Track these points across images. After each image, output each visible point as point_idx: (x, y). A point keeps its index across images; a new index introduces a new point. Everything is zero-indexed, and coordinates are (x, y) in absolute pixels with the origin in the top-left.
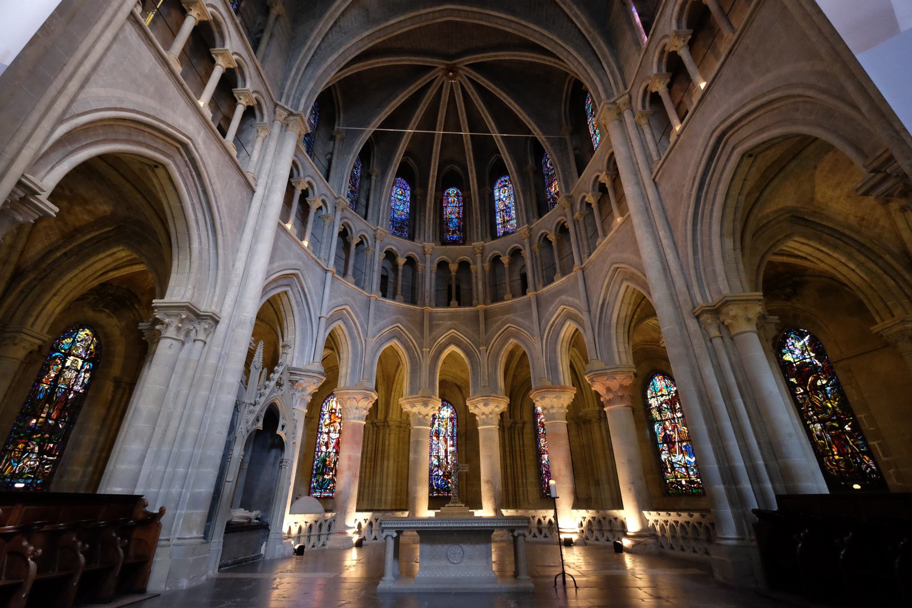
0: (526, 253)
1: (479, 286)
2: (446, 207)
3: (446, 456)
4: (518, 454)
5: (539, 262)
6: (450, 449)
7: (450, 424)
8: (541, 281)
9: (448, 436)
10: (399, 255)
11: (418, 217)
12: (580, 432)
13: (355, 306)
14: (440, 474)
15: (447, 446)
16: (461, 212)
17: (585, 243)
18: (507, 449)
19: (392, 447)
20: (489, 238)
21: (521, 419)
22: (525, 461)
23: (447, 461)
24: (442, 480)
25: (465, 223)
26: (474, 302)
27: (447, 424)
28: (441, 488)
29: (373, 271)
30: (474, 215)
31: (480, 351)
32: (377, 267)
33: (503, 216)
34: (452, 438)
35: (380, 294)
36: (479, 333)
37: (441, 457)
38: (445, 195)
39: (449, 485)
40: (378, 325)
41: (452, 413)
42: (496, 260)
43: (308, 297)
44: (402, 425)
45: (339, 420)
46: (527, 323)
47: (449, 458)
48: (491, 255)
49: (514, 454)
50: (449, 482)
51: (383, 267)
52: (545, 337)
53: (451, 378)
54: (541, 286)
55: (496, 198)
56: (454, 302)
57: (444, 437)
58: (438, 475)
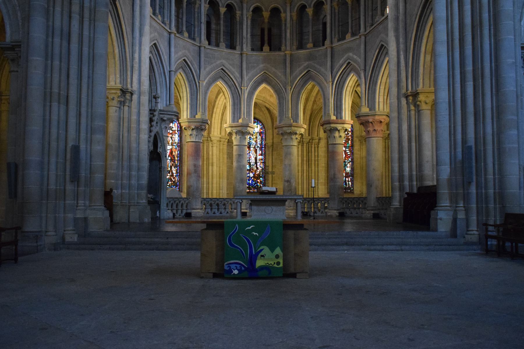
3: (256, 163)
4: (313, 162)
5: (337, 17)
6: (259, 157)
7: (259, 137)
8: (337, 36)
9: (258, 147)
10: (220, 5)
12: (362, 147)
13: (190, 56)
14: (251, 176)
15: (257, 155)
17: (370, 13)
18: (305, 159)
19: (215, 157)
21: (318, 136)
22: (318, 168)
24: (253, 180)
26: (283, 48)
27: (257, 138)
28: (252, 186)
29: (201, 23)
32: (204, 19)
34: (261, 149)
35: (207, 43)
36: (285, 75)
37: (252, 163)
39: (258, 184)
40: (207, 69)
41: (261, 129)
42: (303, 8)
43: (163, 58)
44: (222, 140)
45: (171, 135)
46: (323, 70)
47: (258, 164)
48: (298, 4)
49: (310, 162)
50: (258, 182)
51: (207, 15)
52: (335, 83)
53: (261, 102)
54: (336, 40)
56: (266, 48)
57: (254, 148)
58: (249, 177)
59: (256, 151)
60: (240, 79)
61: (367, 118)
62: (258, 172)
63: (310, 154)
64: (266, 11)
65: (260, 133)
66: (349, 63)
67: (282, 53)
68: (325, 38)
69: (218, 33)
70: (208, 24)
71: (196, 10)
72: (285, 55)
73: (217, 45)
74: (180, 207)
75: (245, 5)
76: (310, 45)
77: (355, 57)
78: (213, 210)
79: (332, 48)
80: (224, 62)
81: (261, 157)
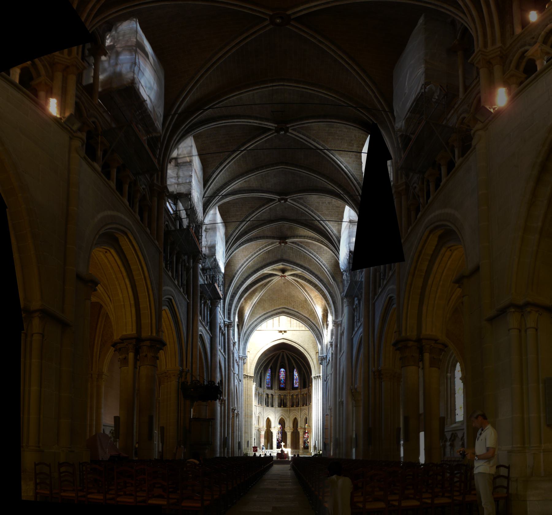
0: (299, 396)
1: (289, 404)
3: (279, 438)
6: (280, 436)
25: (285, 381)
26: (287, 407)
32: (265, 400)
34: (280, 433)
40: (266, 414)
42: (292, 396)
46: (298, 414)
56: (282, 406)
65: (280, 428)
68: (299, 405)
70: (266, 399)
73: (268, 406)
81: (281, 436)
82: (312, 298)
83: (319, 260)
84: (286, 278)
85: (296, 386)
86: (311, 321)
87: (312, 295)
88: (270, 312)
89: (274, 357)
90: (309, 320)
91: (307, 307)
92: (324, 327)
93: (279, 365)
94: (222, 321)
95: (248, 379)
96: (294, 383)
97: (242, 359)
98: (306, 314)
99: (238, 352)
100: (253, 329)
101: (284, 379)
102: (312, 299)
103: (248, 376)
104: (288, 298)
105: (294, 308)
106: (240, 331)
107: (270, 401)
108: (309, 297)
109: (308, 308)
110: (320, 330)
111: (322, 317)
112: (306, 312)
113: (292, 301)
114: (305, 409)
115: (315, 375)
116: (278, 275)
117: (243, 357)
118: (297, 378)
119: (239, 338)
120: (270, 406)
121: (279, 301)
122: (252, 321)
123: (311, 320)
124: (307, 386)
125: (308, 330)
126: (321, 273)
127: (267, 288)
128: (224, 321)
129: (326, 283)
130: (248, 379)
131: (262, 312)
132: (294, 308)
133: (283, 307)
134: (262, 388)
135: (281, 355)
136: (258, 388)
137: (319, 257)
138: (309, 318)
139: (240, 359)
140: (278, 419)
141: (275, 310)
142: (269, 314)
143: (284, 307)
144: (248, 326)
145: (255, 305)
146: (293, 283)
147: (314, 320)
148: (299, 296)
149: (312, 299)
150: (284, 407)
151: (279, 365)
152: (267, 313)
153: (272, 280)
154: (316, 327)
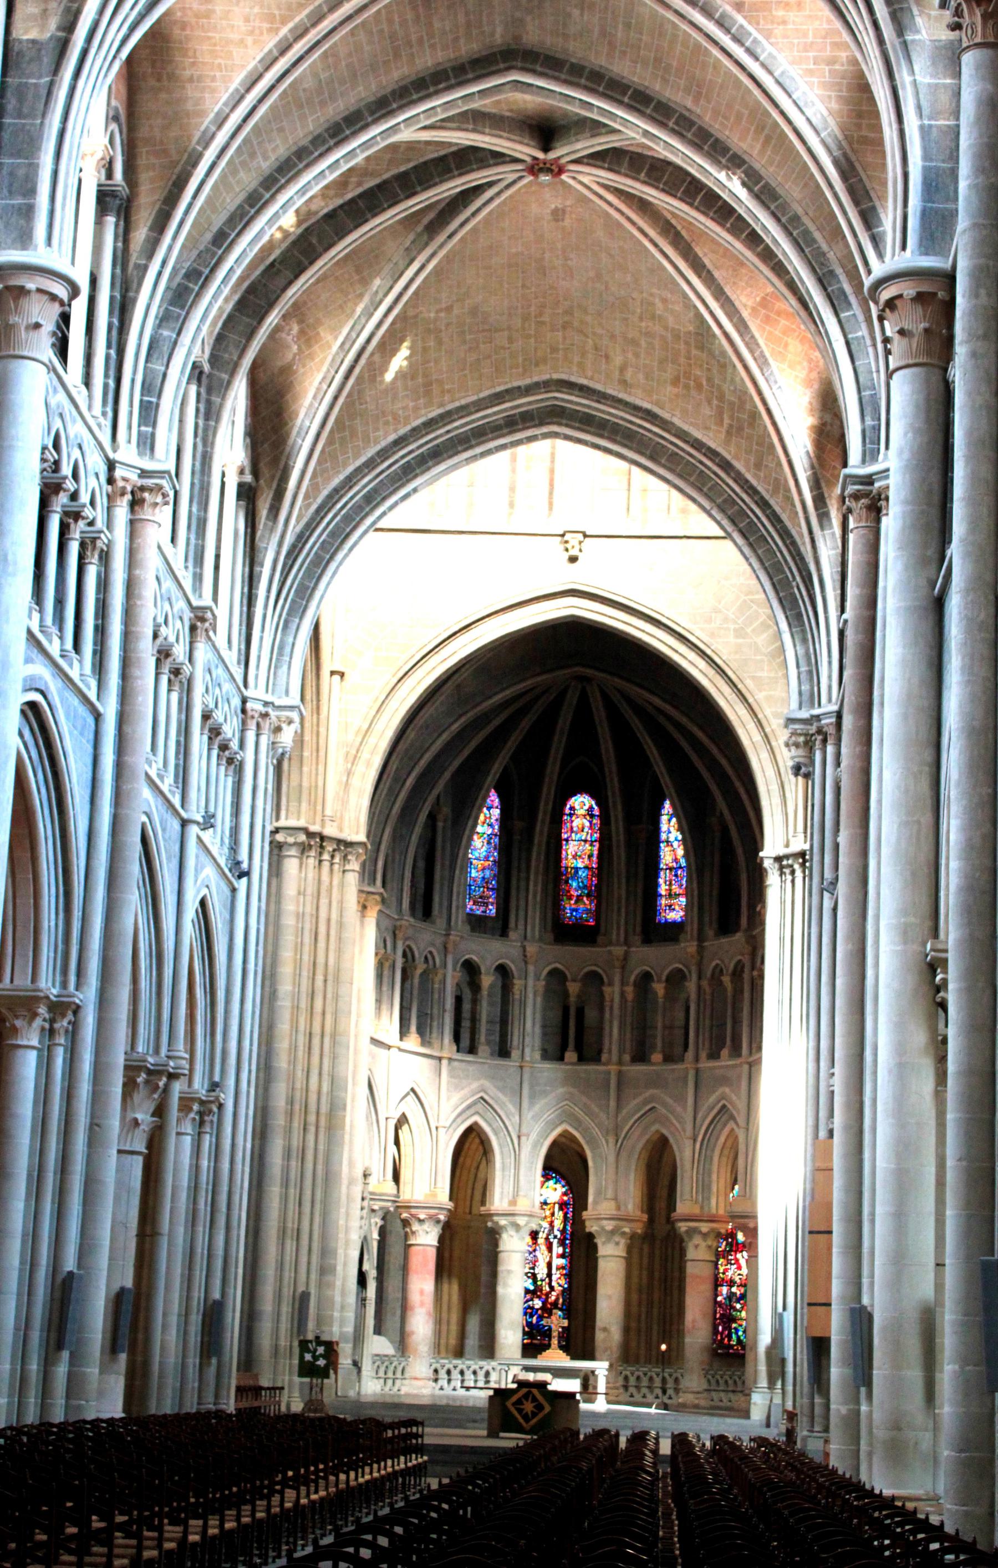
2: (567, 840)
3: (549, 1275)
7: (559, 1215)
9: (555, 1237)
10: (483, 970)
11: (514, 882)
16: (596, 853)
18: (657, 1274)
20: (637, 939)
23: (550, 1284)
25: (600, 880)
26: (604, 1057)
27: (553, 1214)
29: (444, 1011)
30: (616, 886)
31: (607, 1142)
32: (449, 1003)
33: (670, 885)
34: (562, 1243)
37: (539, 1277)
38: (567, 811)
41: (565, 1194)
42: (646, 978)
46: (679, 1109)
47: (554, 1278)
48: (636, 972)
52: (700, 1138)
55: (663, 836)
56: (571, 1056)
57: (547, 1239)
58: (532, 1308)
59: (550, 1247)
60: (517, 1118)
61: (746, 1220)
62: (553, 1298)
63: (669, 1264)
64: (574, 980)
65: (563, 1205)
66: (724, 1106)
67: (601, 1068)
69: (474, 1020)
70: (458, 1000)
71: (436, 986)
72: (609, 1073)
73: (472, 1050)
74: (390, 1374)
75: (531, 968)
76: (657, 1057)
77: (734, 1098)
78: (453, 1384)
79: (697, 1071)
80: (487, 1084)
81: (562, 1262)
82: (745, 314)
83: (749, 51)
84: (564, 177)
85: (675, 916)
86: (739, 478)
87: (744, 299)
88: (463, 411)
89: (522, 712)
90: (726, 466)
91: (709, 380)
92: (823, 516)
93: (553, 770)
94: (96, 463)
95: (326, 856)
96: (657, 895)
97: (266, 726)
98: (707, 428)
99: (238, 673)
100: (347, 519)
101: (586, 868)
102: (742, 327)
103: (322, 838)
104: (589, 319)
105: (624, 383)
106: (259, 534)
107: (486, 1010)
108: (722, 307)
109: (719, 387)
110: (802, 536)
111: (810, 448)
112: (707, 411)
113: (613, 337)
114: (724, 1081)
115: (787, 846)
116: (516, 161)
117: (273, 713)
118: (676, 860)
119: (251, 580)
120: (483, 1049)
121: (529, 337)
122: (345, 465)
123: (738, 465)
124: (744, 921)
125: (722, 534)
126: (768, 139)
127: (441, 246)
128: (111, 466)
129: (800, 211)
130: (326, 856)
131: (416, 409)
132: (624, 383)
133: (555, 376)
134: (433, 923)
135: (572, 698)
136: (408, 920)
137: (750, 28)
138: (728, 457)
139: (252, 725)
140: (536, 1145)
141: (498, 398)
142: (459, 426)
143: (564, 376)
144: (319, 500)
145: (363, 361)
146: (612, 211)
147: (758, 466)
148: (659, 305)
149: (742, 327)
150: (582, 1059)
151: (553, 770)
152: (446, 417)
153: (477, 190)
154: (775, 519)
